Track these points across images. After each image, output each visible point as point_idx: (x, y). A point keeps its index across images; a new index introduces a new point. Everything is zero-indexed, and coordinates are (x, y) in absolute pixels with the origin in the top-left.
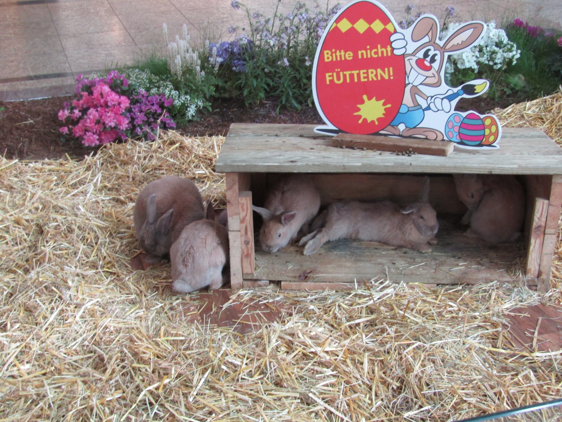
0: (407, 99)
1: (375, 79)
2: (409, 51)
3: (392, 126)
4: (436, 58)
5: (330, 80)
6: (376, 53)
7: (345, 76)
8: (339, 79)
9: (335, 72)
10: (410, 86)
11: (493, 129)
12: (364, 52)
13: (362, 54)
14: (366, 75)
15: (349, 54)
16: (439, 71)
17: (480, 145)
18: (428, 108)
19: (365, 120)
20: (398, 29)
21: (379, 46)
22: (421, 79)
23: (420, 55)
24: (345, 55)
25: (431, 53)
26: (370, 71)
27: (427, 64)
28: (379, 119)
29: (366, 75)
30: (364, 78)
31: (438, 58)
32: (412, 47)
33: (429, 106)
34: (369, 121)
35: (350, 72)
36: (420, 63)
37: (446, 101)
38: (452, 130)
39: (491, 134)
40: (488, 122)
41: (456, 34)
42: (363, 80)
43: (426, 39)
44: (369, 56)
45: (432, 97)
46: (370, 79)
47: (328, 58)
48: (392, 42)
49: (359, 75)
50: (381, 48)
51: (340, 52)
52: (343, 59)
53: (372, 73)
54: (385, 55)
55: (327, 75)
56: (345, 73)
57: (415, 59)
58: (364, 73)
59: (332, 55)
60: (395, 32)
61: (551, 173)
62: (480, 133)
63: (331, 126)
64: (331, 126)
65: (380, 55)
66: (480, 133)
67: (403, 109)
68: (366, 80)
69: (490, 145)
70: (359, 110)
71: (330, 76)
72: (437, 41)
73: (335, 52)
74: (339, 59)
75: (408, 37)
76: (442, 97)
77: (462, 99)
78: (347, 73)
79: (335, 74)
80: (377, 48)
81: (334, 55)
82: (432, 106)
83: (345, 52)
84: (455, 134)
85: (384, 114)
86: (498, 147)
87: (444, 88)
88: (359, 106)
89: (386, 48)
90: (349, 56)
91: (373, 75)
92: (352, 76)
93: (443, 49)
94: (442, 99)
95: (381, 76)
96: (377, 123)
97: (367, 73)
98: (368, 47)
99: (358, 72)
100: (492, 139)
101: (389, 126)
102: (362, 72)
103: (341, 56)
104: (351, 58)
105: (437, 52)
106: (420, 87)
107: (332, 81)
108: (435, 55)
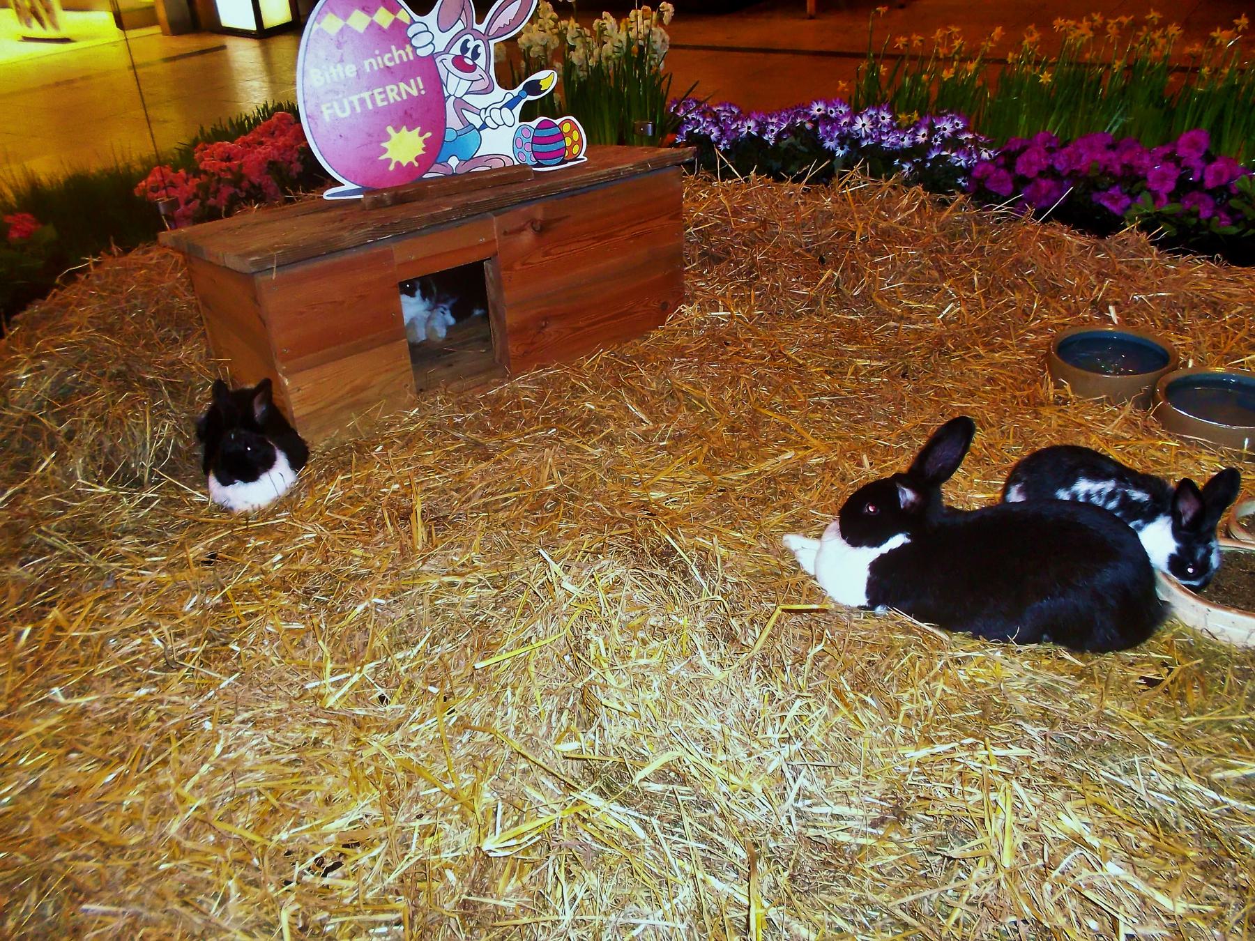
0: (452, 121)
1: (399, 99)
2: (440, 47)
3: (440, 164)
4: (479, 50)
6: (391, 59)
7: (351, 103)
10: (452, 98)
11: (575, 136)
12: (373, 60)
14: (383, 96)
16: (487, 71)
17: (566, 162)
18: (484, 126)
19: (398, 164)
20: (416, 18)
21: (393, 48)
22: (465, 85)
23: (456, 50)
25: (471, 45)
26: (388, 88)
27: (469, 62)
28: (417, 159)
29: (383, 96)
30: (383, 100)
31: (481, 50)
32: (442, 40)
33: (484, 122)
34: (405, 164)
36: (458, 62)
37: (505, 110)
38: (522, 150)
39: (574, 143)
40: (566, 128)
41: (501, 9)
42: (380, 104)
43: (460, 26)
45: (486, 109)
46: (392, 101)
48: (411, 39)
50: (397, 50)
57: (449, 58)
58: (380, 93)
60: (413, 22)
61: (473, 258)
62: (560, 145)
63: (349, 186)
64: (349, 186)
65: (398, 61)
66: (560, 145)
67: (449, 136)
68: (385, 103)
69: (575, 159)
70: (385, 151)
72: (476, 26)
75: (434, 27)
76: (499, 106)
77: (527, 101)
80: (390, 51)
82: (489, 122)
84: (528, 154)
85: (424, 149)
86: (586, 159)
87: (499, 94)
88: (384, 145)
89: (404, 49)
93: (486, 37)
94: (500, 109)
96: (416, 164)
97: (385, 92)
98: (377, 52)
100: (576, 149)
101: (436, 165)
102: (376, 91)
105: (479, 42)
106: (466, 98)
107: (334, 116)
108: (477, 46)
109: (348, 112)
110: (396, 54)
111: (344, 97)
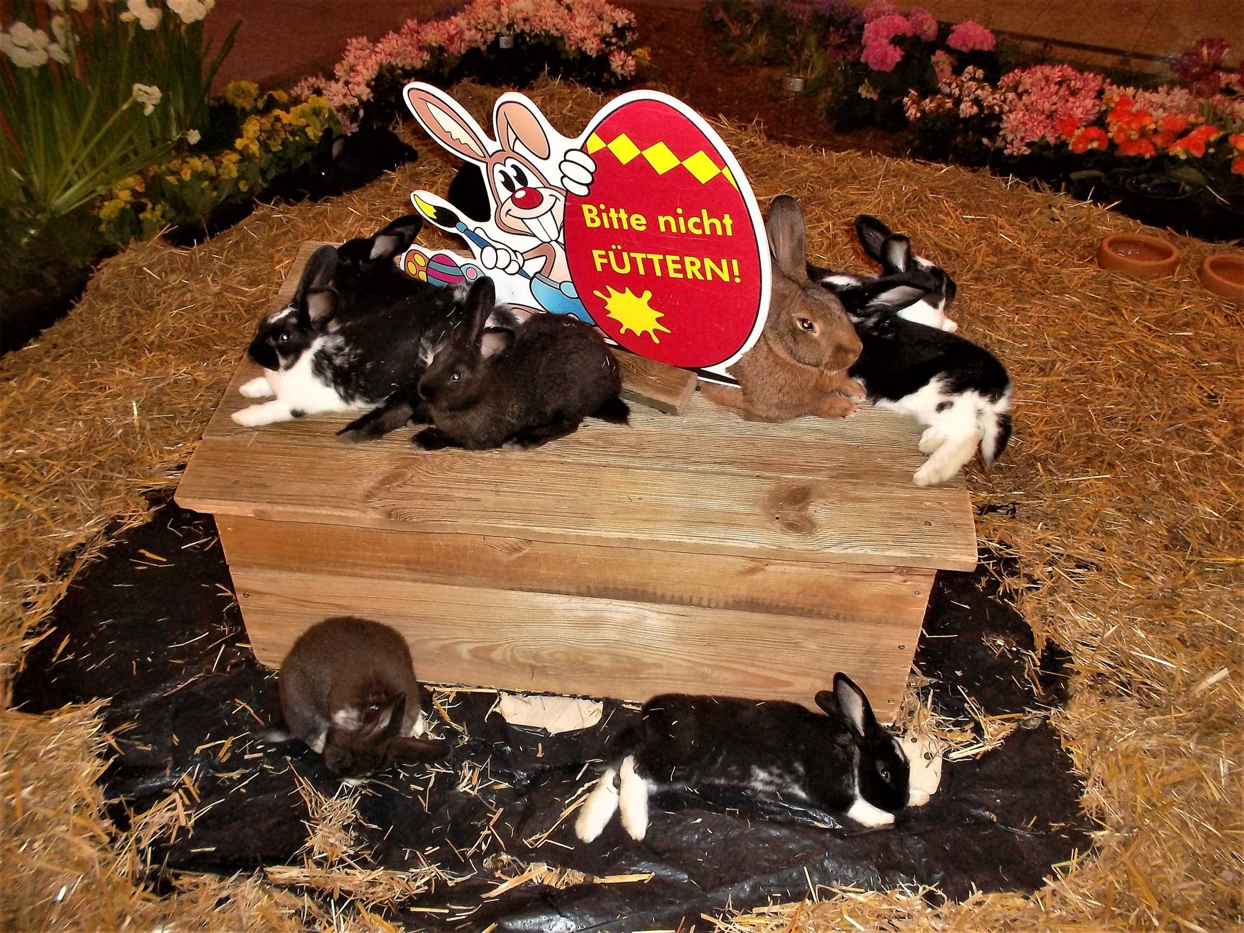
1: (700, 277)
6: (696, 225)
7: (633, 262)
8: (621, 264)
13: (667, 224)
14: (679, 266)
15: (637, 219)
21: (704, 212)
24: (628, 220)
26: (687, 260)
29: (679, 266)
30: (676, 271)
35: (644, 256)
46: (690, 276)
47: (593, 221)
49: (663, 264)
52: (626, 227)
55: (596, 253)
56: (632, 255)
58: (674, 262)
59: (599, 215)
65: (708, 232)
68: (680, 276)
73: (608, 212)
78: (639, 257)
79: (611, 254)
81: (604, 215)
89: (721, 219)
90: (638, 222)
91: (696, 269)
92: (648, 264)
97: (682, 262)
99: (661, 257)
102: (669, 258)
103: (619, 220)
104: (643, 228)
107: (606, 267)
109: (627, 269)
110: (707, 223)
111: (623, 250)
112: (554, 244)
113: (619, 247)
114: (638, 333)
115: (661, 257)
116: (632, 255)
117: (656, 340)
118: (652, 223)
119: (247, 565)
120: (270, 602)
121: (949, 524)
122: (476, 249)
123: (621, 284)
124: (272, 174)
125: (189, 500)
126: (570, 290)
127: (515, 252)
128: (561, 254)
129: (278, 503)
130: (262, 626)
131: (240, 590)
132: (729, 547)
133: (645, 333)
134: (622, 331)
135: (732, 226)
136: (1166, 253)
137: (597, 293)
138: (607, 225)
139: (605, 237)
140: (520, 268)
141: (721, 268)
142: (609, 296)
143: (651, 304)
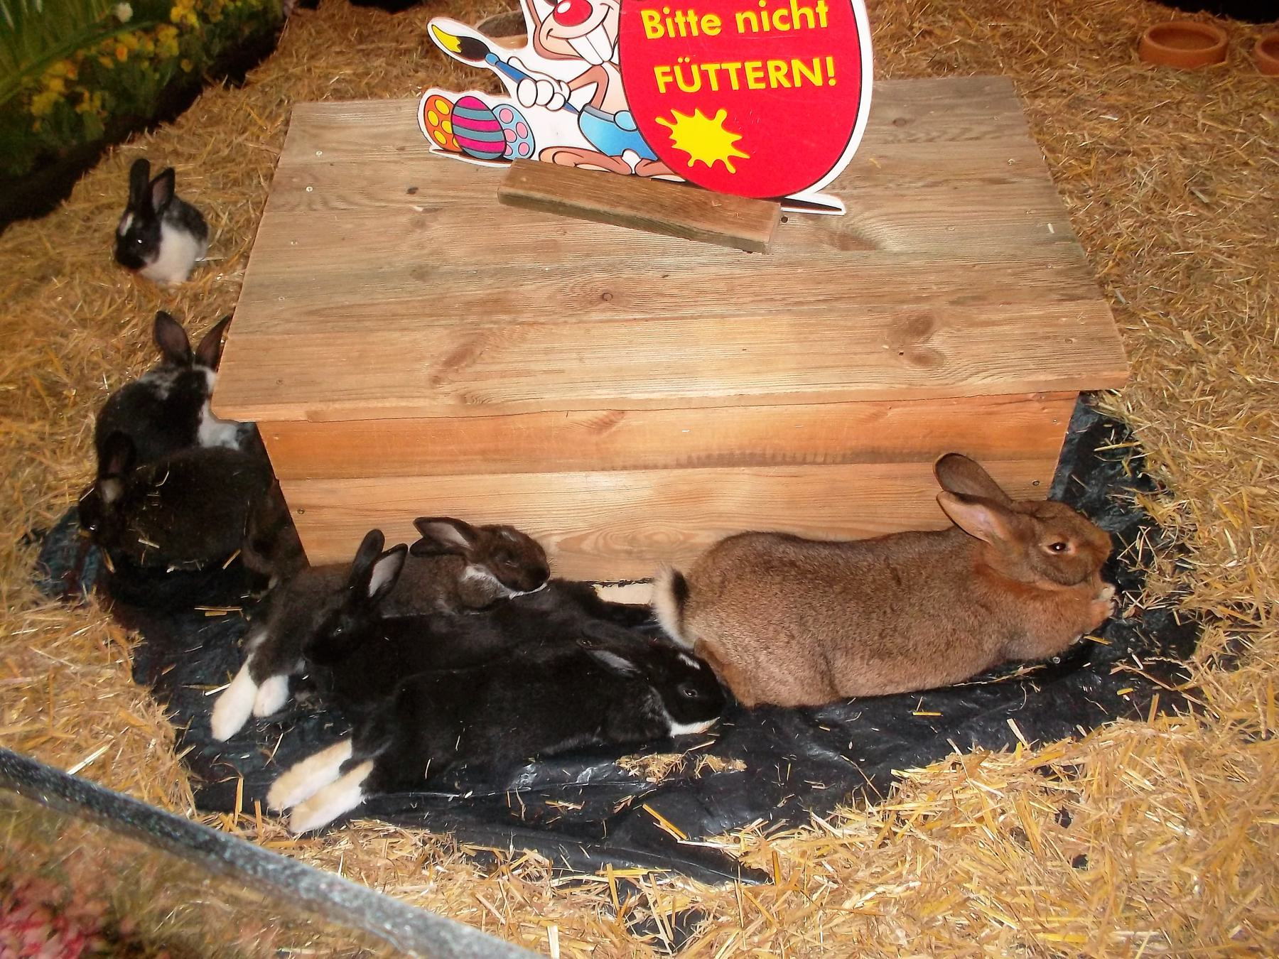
1: (786, 84)
5: (667, 84)
6: (784, 19)
7: (704, 75)
8: (689, 80)
9: (677, 63)
12: (751, 15)
13: (747, 22)
15: (710, 21)
26: (771, 64)
29: (761, 74)
30: (757, 80)
35: (717, 66)
42: (752, 85)
44: (767, 28)
46: (774, 85)
47: (655, 30)
49: (741, 74)
50: (800, 5)
51: (685, 14)
52: (695, 32)
53: (778, 69)
54: (811, 25)
55: (659, 70)
56: (704, 67)
58: (755, 69)
59: (663, 22)
65: (797, 25)
68: (762, 86)
71: (664, 74)
73: (673, 15)
74: (683, 33)
78: (711, 68)
79: (677, 69)
81: (669, 21)
83: (700, 15)
90: (711, 25)
91: (781, 76)
92: (723, 76)
95: (803, 77)
97: (764, 68)
99: (738, 65)
102: (749, 66)
103: (688, 25)
104: (717, 32)
107: (672, 86)
109: (697, 86)
112: (607, 66)
113: (687, 60)
114: (710, 164)
115: (738, 65)
116: (704, 67)
117: (732, 169)
118: (729, 24)
119: (298, 478)
120: (328, 516)
121: (1092, 339)
122: (510, 84)
123: (688, 104)
124: (217, 48)
125: (229, 409)
126: (627, 121)
127: (559, 82)
128: (615, 77)
129: (334, 401)
130: (321, 543)
131: (294, 506)
132: (852, 392)
133: (719, 163)
134: (691, 163)
135: (827, 13)
136: (1212, 40)
137: (660, 120)
138: (672, 34)
139: (669, 49)
140: (566, 102)
141: (812, 69)
142: (674, 121)
143: (727, 125)
